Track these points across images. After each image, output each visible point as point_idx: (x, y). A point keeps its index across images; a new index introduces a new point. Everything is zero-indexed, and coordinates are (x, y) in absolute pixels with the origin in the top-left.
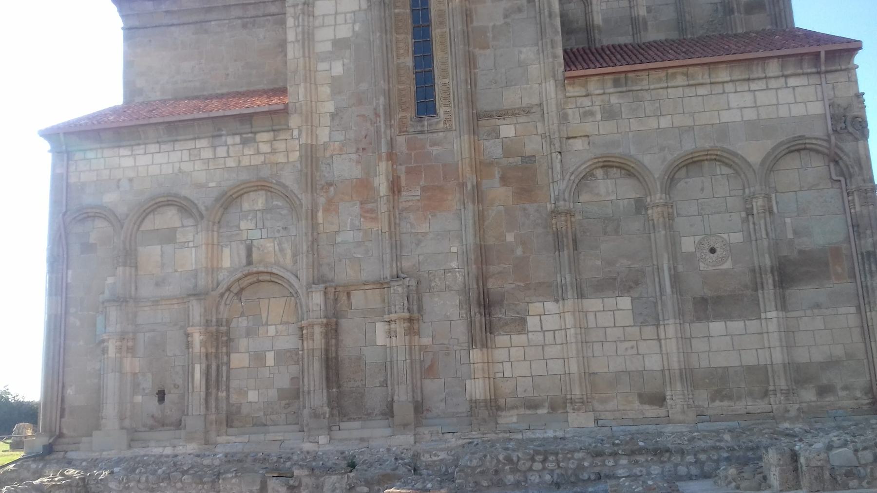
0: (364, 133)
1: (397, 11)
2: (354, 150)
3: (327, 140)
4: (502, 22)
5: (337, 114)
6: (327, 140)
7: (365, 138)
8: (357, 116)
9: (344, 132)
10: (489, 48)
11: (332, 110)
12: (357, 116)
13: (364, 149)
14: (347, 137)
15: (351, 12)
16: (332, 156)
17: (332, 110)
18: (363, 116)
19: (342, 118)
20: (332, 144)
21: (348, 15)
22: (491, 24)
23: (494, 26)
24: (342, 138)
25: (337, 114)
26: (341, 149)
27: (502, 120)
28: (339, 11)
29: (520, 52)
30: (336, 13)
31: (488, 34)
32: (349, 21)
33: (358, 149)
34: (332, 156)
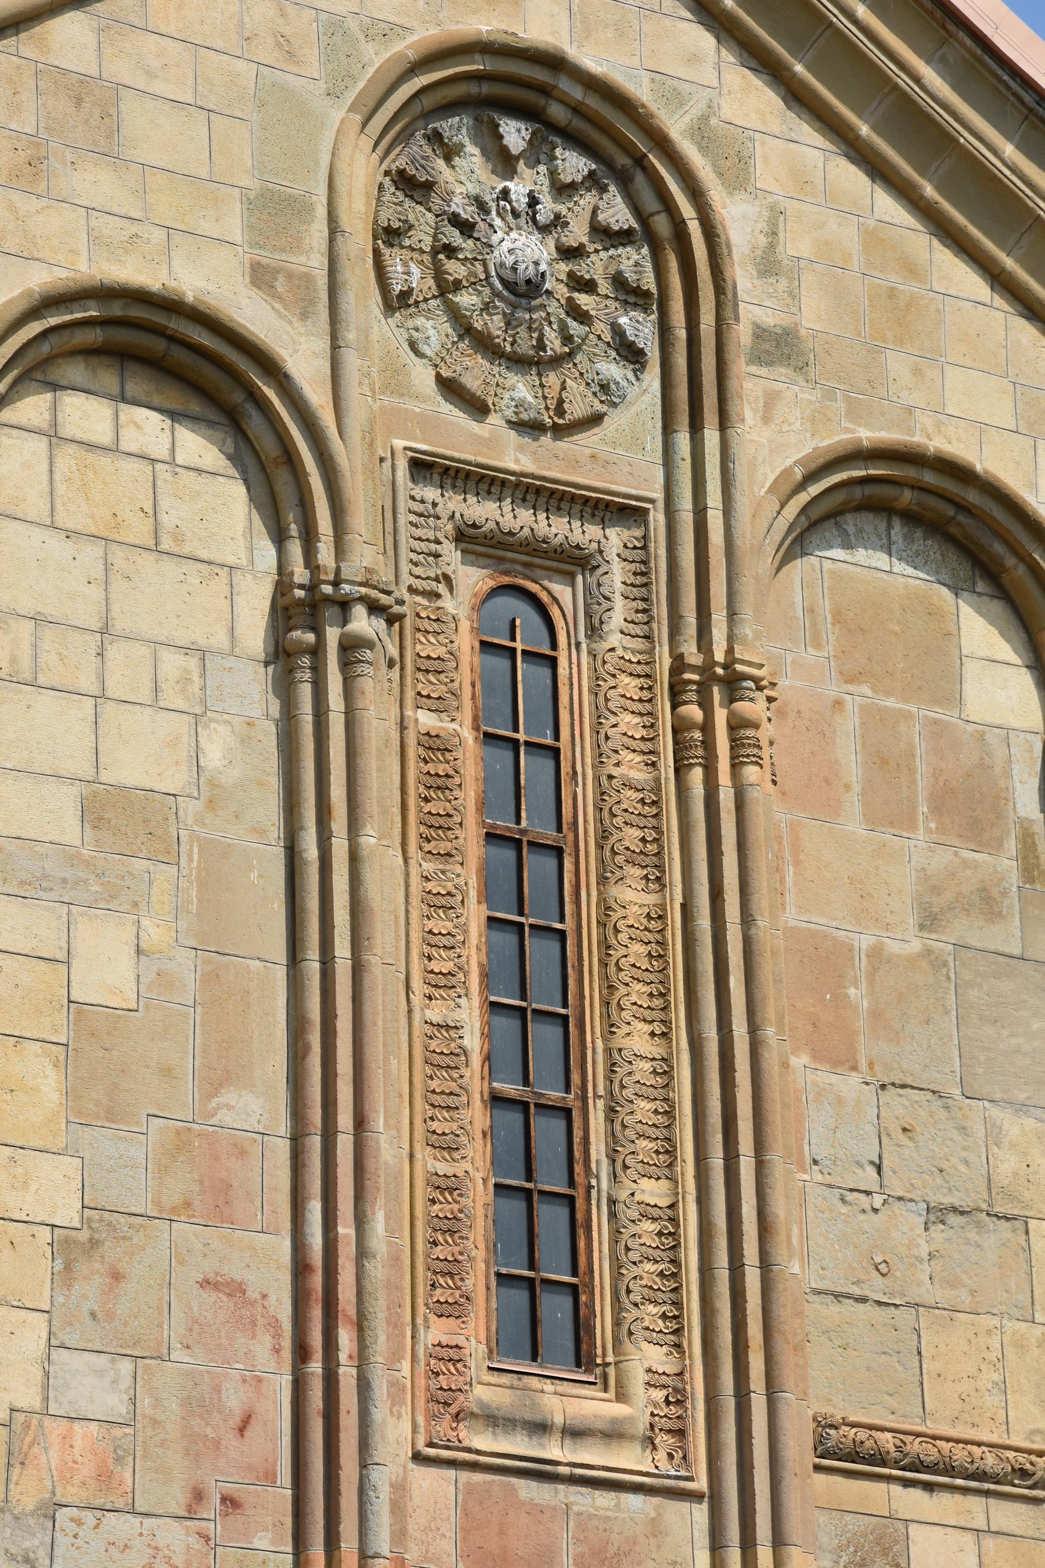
0: (234, 1400)
1: (426, 720)
2: (177, 1500)
3: (30, 1399)
4: (915, 946)
5: (94, 1243)
6: (30, 1399)
7: (242, 1430)
8: (205, 1283)
9: (126, 1366)
10: (854, 1068)
11: (68, 1214)
12: (205, 1283)
13: (230, 1502)
14: (145, 1403)
15: (187, 650)
16: (50, 1510)
17: (68, 1214)
18: (236, 1290)
19: (117, 1276)
20: (54, 1429)
21: (172, 663)
22: (866, 942)
23: (876, 954)
24: (116, 1405)
25: (94, 1243)
26: (105, 1477)
27: (917, 1494)
28: (119, 624)
29: (994, 1135)
30: (105, 630)
31: (852, 991)
32: (171, 697)
33: (199, 1495)
34: (50, 1510)
